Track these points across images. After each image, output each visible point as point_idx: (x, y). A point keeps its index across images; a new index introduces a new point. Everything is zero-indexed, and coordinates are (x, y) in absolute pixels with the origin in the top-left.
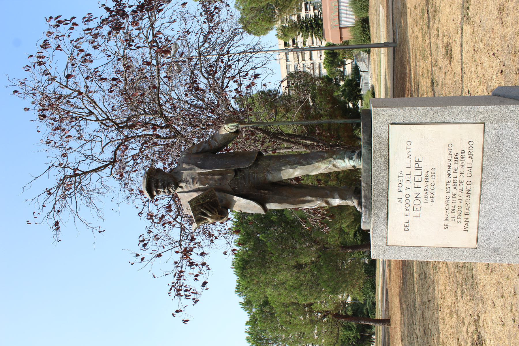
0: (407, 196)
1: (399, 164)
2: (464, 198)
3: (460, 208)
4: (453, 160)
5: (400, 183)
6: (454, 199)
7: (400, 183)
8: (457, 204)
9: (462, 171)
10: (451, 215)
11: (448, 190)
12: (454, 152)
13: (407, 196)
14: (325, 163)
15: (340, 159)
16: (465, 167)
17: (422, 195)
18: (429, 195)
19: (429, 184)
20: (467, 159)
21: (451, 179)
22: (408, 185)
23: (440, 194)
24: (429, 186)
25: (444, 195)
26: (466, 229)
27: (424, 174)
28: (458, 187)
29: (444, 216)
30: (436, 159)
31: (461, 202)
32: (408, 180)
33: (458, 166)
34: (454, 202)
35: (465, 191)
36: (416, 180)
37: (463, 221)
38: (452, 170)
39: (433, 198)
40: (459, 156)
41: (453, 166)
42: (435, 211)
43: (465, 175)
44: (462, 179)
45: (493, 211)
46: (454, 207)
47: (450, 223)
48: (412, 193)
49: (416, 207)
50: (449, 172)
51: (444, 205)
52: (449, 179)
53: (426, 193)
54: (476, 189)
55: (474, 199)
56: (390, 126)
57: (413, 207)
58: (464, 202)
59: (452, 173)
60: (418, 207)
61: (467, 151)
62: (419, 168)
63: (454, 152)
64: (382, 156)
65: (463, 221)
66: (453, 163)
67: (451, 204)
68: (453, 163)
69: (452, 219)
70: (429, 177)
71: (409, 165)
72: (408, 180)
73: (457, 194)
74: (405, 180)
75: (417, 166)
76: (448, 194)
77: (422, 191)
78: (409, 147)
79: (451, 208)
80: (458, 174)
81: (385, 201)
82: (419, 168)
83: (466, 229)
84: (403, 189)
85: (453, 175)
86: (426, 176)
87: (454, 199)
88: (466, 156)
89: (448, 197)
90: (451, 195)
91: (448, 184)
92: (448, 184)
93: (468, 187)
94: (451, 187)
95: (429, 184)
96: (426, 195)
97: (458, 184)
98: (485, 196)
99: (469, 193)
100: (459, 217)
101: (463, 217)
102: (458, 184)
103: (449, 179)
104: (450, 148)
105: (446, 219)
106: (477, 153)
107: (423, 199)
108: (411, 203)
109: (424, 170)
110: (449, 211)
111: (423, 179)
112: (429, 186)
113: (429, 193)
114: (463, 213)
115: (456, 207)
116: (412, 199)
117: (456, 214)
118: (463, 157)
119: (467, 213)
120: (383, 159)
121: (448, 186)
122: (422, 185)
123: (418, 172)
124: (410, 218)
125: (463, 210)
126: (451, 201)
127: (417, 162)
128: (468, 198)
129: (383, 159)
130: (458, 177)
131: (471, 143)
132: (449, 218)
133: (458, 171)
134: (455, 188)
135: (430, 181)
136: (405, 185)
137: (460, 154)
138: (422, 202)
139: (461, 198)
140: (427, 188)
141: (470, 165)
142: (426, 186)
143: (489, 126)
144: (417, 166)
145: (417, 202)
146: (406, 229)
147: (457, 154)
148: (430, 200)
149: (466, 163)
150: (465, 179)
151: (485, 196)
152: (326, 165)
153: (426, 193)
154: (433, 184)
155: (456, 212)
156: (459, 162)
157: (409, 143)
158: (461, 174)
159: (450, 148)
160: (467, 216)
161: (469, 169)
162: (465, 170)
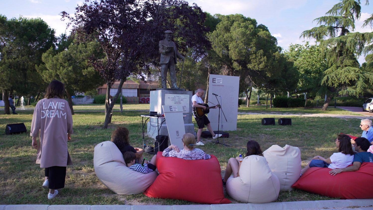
1: (182, 96)
5: (178, 97)
7: (178, 97)
57: (173, 99)
62: (181, 101)
77: (176, 101)
82: (181, 101)
84: (177, 97)
107: (175, 101)
116: (175, 99)
124: (171, 99)
143: (188, 114)
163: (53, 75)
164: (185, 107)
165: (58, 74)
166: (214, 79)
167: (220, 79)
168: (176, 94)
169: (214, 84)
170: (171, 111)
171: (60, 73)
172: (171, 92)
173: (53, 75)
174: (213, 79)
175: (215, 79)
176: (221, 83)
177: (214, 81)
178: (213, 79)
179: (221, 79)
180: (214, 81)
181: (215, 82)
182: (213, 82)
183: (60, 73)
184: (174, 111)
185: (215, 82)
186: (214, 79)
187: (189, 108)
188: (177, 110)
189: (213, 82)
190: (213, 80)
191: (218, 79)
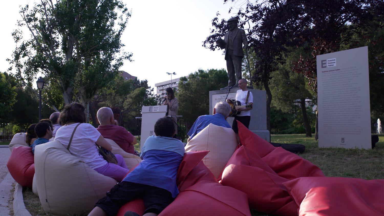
166: (324, 62)
167: (333, 59)
174: (322, 61)
175: (325, 60)
176: (335, 65)
177: (324, 65)
178: (322, 61)
179: (335, 59)
180: (324, 65)
181: (325, 67)
182: (322, 67)
184: (153, 111)
185: (325, 67)
186: (324, 62)
188: (158, 111)
189: (322, 67)
190: (322, 64)
191: (330, 60)
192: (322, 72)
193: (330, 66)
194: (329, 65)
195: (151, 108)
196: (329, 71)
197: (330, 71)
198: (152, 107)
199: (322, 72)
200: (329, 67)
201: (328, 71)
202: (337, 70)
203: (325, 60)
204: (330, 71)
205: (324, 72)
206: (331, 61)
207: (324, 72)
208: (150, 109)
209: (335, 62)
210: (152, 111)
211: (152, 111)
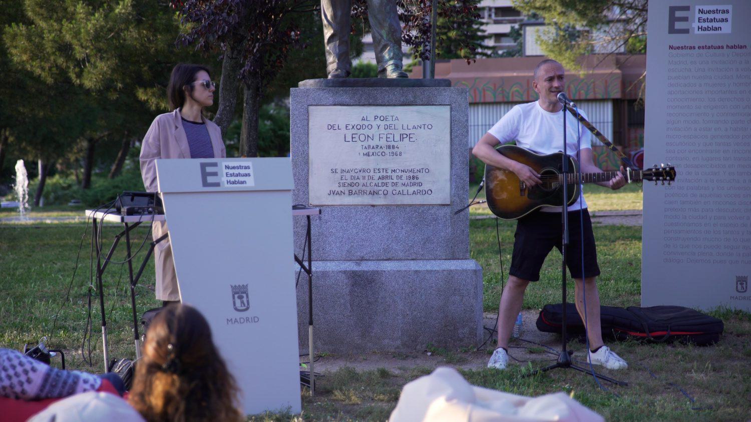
0: (370, 127)
2: (368, 189)
3: (357, 185)
4: (411, 174)
5: (385, 119)
6: (367, 178)
7: (385, 119)
8: (361, 181)
9: (399, 184)
10: (348, 176)
11: (377, 171)
12: (420, 175)
13: (370, 127)
14: (388, 35)
15: (394, 54)
16: (404, 188)
17: (372, 143)
18: (371, 151)
19: (384, 150)
20: (411, 189)
21: (389, 174)
22: (382, 128)
23: (372, 163)
24: (381, 150)
25: (372, 166)
26: (333, 193)
27: (395, 144)
28: (380, 181)
29: (347, 168)
30: (411, 156)
31: (364, 185)
32: (387, 127)
33: (404, 180)
34: (364, 178)
35: (376, 188)
36: (388, 136)
37: (342, 189)
38: (400, 174)
39: (368, 155)
40: (415, 180)
41: (405, 175)
42: (352, 157)
43: (395, 188)
44: (389, 185)
45: (353, 220)
46: (358, 178)
47: (338, 175)
48: (374, 131)
49: (357, 136)
50: (398, 171)
51: (359, 167)
52: (390, 171)
53: (373, 148)
54: (379, 201)
55: (367, 200)
56: (449, 107)
57: (356, 133)
58: (364, 188)
59: (396, 174)
60: (357, 139)
61: (421, 188)
62: (402, 138)
63: (420, 175)
64: (415, 97)
65: (342, 189)
66: (408, 174)
67: (362, 174)
68: (408, 174)
69: (344, 177)
70: (391, 150)
71: (405, 127)
72: (387, 127)
73: (372, 181)
74: (388, 123)
75: (405, 136)
76: (372, 171)
77: (376, 142)
78: (426, 126)
79: (356, 175)
80: (395, 181)
81: (363, 102)
82: (402, 138)
83: (333, 193)
84: (378, 122)
85: (394, 175)
86: (393, 147)
87: (367, 178)
88: (416, 188)
89: (369, 171)
90: (372, 174)
91: (384, 170)
92: (384, 170)
93: (381, 192)
94: (381, 174)
95: (384, 150)
96: (371, 147)
97: (384, 181)
98: (370, 211)
99: (374, 193)
100: (346, 185)
101: (346, 189)
102: (384, 181)
103: (390, 171)
104: (424, 170)
105: (343, 171)
106: (418, 200)
107: (366, 144)
108: (361, 131)
109: (400, 144)
110: (353, 174)
111: (389, 143)
112: (381, 150)
113: (373, 150)
114: (350, 188)
115: (358, 181)
116: (366, 132)
117: (349, 181)
118: (414, 184)
119: (350, 193)
120: (412, 99)
121: (381, 171)
122: (383, 142)
123: (397, 138)
124: (344, 131)
125: (354, 189)
126: (364, 174)
127: (409, 136)
128: (368, 193)
129: (412, 99)
130: (392, 181)
131: (430, 192)
132: (345, 174)
133: (399, 181)
134: (379, 178)
135: (387, 151)
136: (382, 123)
137: (418, 181)
138: (363, 143)
139: (368, 185)
140: (379, 148)
141: (405, 192)
142: (381, 147)
144: (405, 136)
145: (362, 138)
146: (330, 127)
147: (417, 178)
148: (366, 151)
149: (408, 188)
150: (390, 189)
151: (370, 211)
152: (385, 36)
153: (373, 148)
154: (383, 154)
155: (351, 181)
156: (409, 181)
157: (430, 127)
158: (396, 184)
159: (424, 170)
160: (347, 192)
161: (401, 192)
162: (400, 188)
163: (49, 47)
164: (428, 171)
165: (68, 37)
166: (678, 14)
167: (721, 7)
168: (370, 105)
169: (678, 40)
170: (205, 184)
171: (77, 34)
172: (345, 98)
173: (49, 47)
175: (687, 8)
177: (678, 25)
178: (673, 10)
179: (729, 7)
180: (678, 25)
181: (686, 31)
182: (672, 30)
183: (77, 34)
184: (226, 186)
185: (686, 31)
186: (678, 14)
187: (448, 177)
188: (250, 183)
189: (672, 30)
190: (673, 20)
192: (671, 47)
193: (705, 29)
194: (700, 25)
195: (209, 169)
196: (699, 48)
197: (703, 48)
198: (215, 165)
199: (671, 47)
200: (700, 32)
201: (694, 48)
202: (732, 47)
203: (687, 8)
204: (703, 48)
205: (678, 48)
206: (717, 11)
207: (678, 48)
208: (205, 175)
209: (727, 20)
210: (218, 185)
211: (218, 185)
